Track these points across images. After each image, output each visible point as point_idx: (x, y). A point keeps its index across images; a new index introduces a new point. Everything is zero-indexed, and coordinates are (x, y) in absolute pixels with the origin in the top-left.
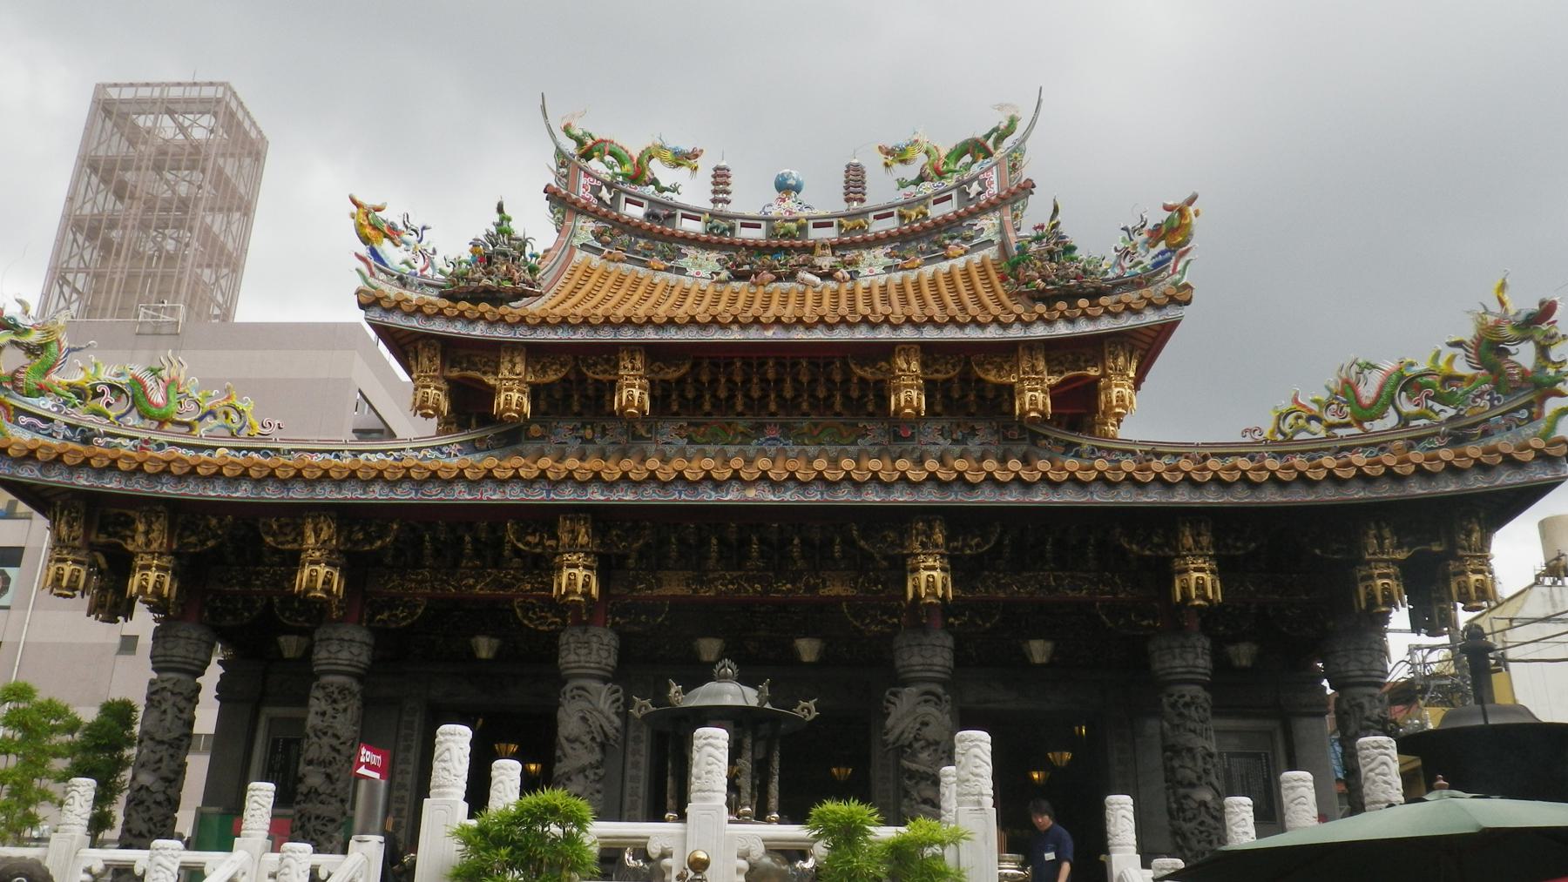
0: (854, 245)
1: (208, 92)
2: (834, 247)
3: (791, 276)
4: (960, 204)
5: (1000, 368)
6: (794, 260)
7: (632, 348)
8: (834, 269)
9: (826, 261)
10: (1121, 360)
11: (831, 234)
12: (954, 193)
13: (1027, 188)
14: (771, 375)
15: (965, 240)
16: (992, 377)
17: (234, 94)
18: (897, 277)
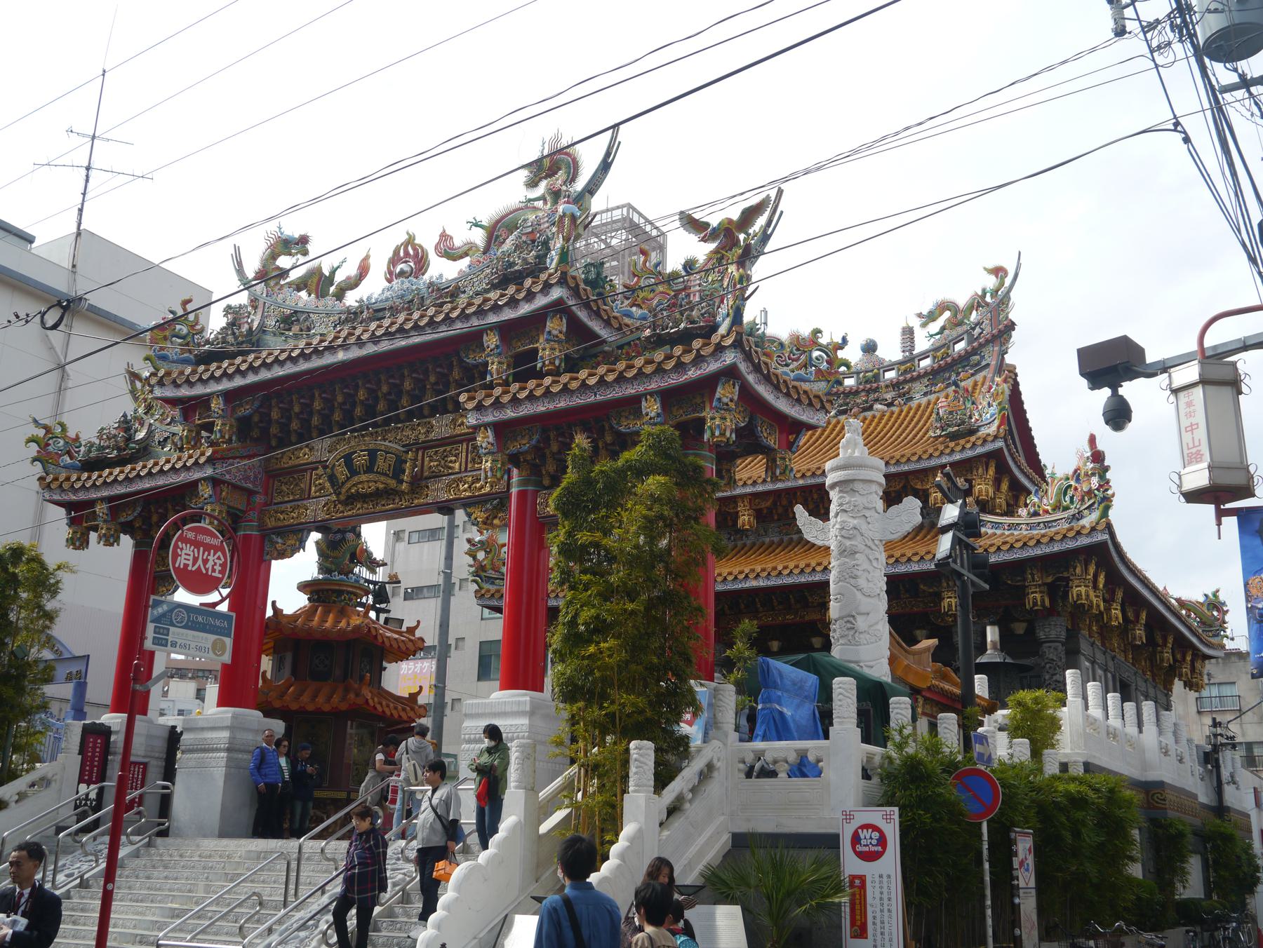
0: (905, 381)
1: (617, 214)
2: (895, 385)
3: (870, 408)
4: (969, 343)
5: (922, 481)
6: (872, 397)
7: (742, 496)
8: (894, 399)
9: (889, 396)
10: (980, 470)
11: (891, 375)
12: (965, 336)
13: (1012, 326)
14: (815, 496)
15: (973, 367)
16: (919, 486)
17: (634, 209)
18: (932, 397)
